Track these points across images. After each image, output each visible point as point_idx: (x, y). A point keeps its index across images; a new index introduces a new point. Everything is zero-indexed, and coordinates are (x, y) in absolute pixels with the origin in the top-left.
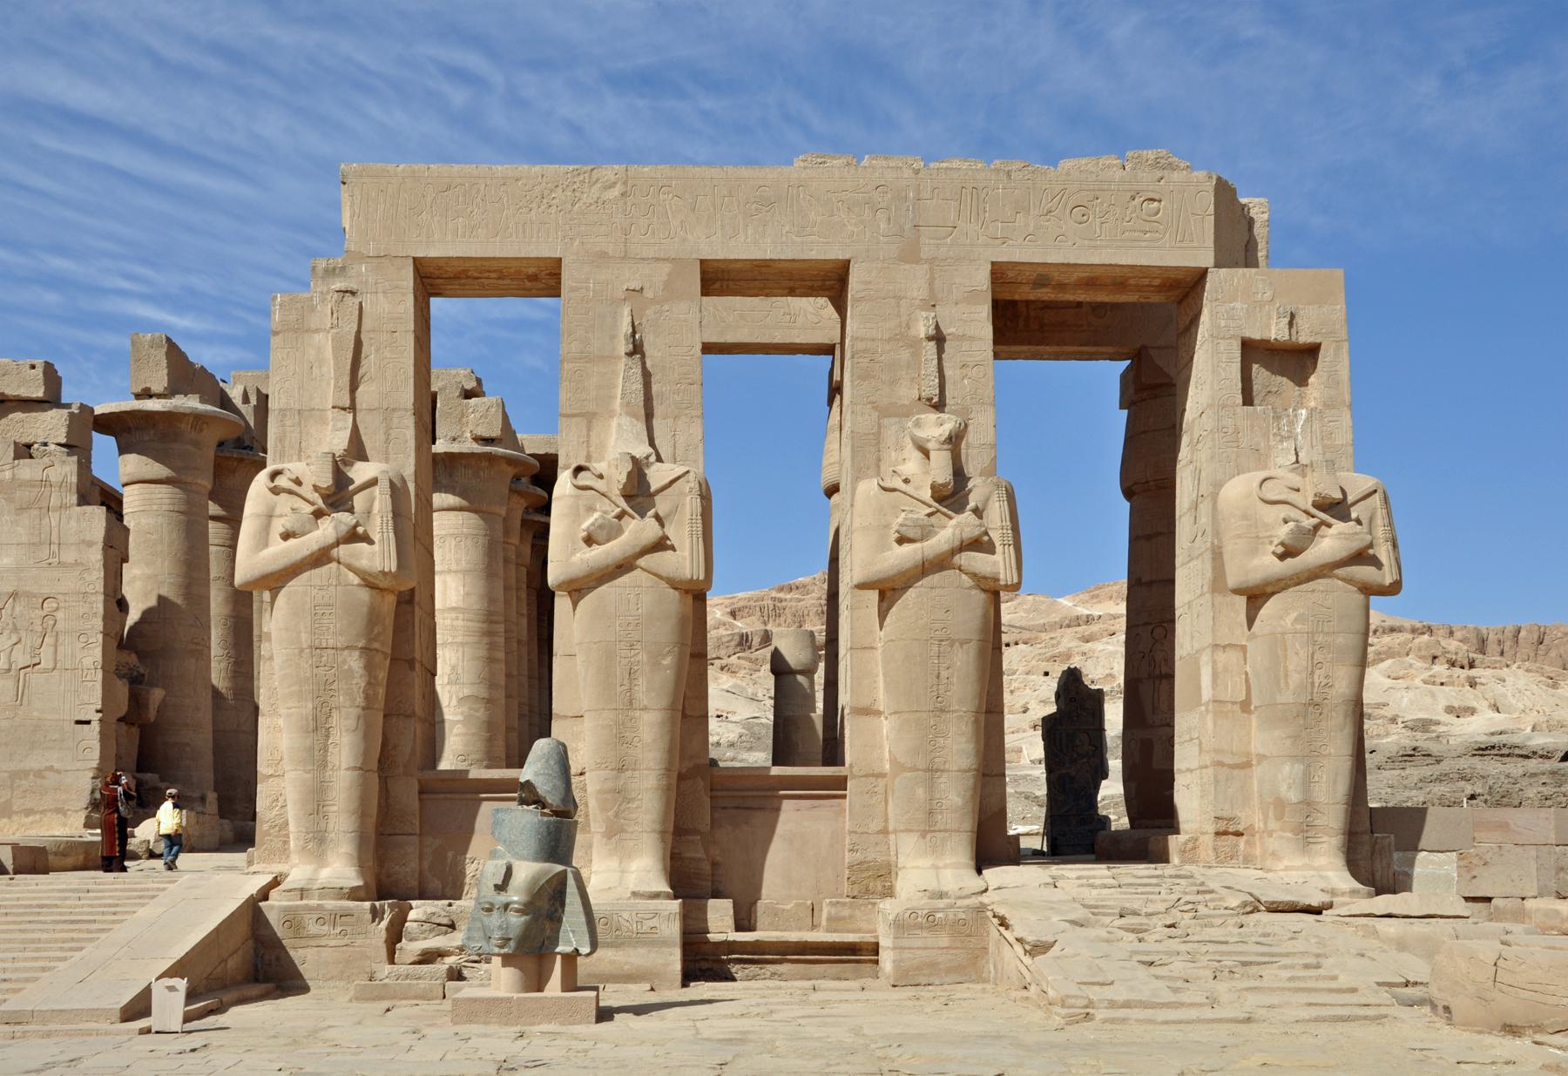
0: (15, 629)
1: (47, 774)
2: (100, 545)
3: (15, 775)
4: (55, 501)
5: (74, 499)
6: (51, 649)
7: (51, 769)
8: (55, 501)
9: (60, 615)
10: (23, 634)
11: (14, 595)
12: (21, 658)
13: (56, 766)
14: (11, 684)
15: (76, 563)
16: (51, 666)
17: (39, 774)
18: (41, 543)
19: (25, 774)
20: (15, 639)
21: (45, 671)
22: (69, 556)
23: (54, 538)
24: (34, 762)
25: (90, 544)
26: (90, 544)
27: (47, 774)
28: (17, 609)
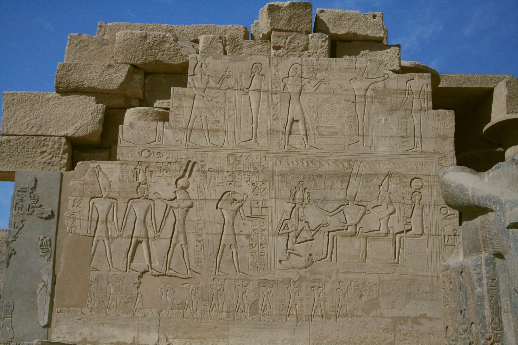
0: (391, 202)
1: (422, 321)
2: (452, 140)
3: (397, 321)
4: (415, 105)
5: (430, 104)
6: (420, 218)
7: (424, 316)
8: (415, 105)
9: (424, 192)
10: (397, 206)
11: (389, 175)
12: (396, 225)
13: (429, 315)
14: (389, 245)
15: (435, 153)
16: (420, 232)
17: (416, 321)
18: (407, 136)
19: (404, 320)
20: (391, 210)
21: (415, 236)
22: (429, 146)
23: (417, 133)
24: (411, 310)
25: (445, 138)
26: (445, 138)
27: (422, 321)
28: (392, 186)
